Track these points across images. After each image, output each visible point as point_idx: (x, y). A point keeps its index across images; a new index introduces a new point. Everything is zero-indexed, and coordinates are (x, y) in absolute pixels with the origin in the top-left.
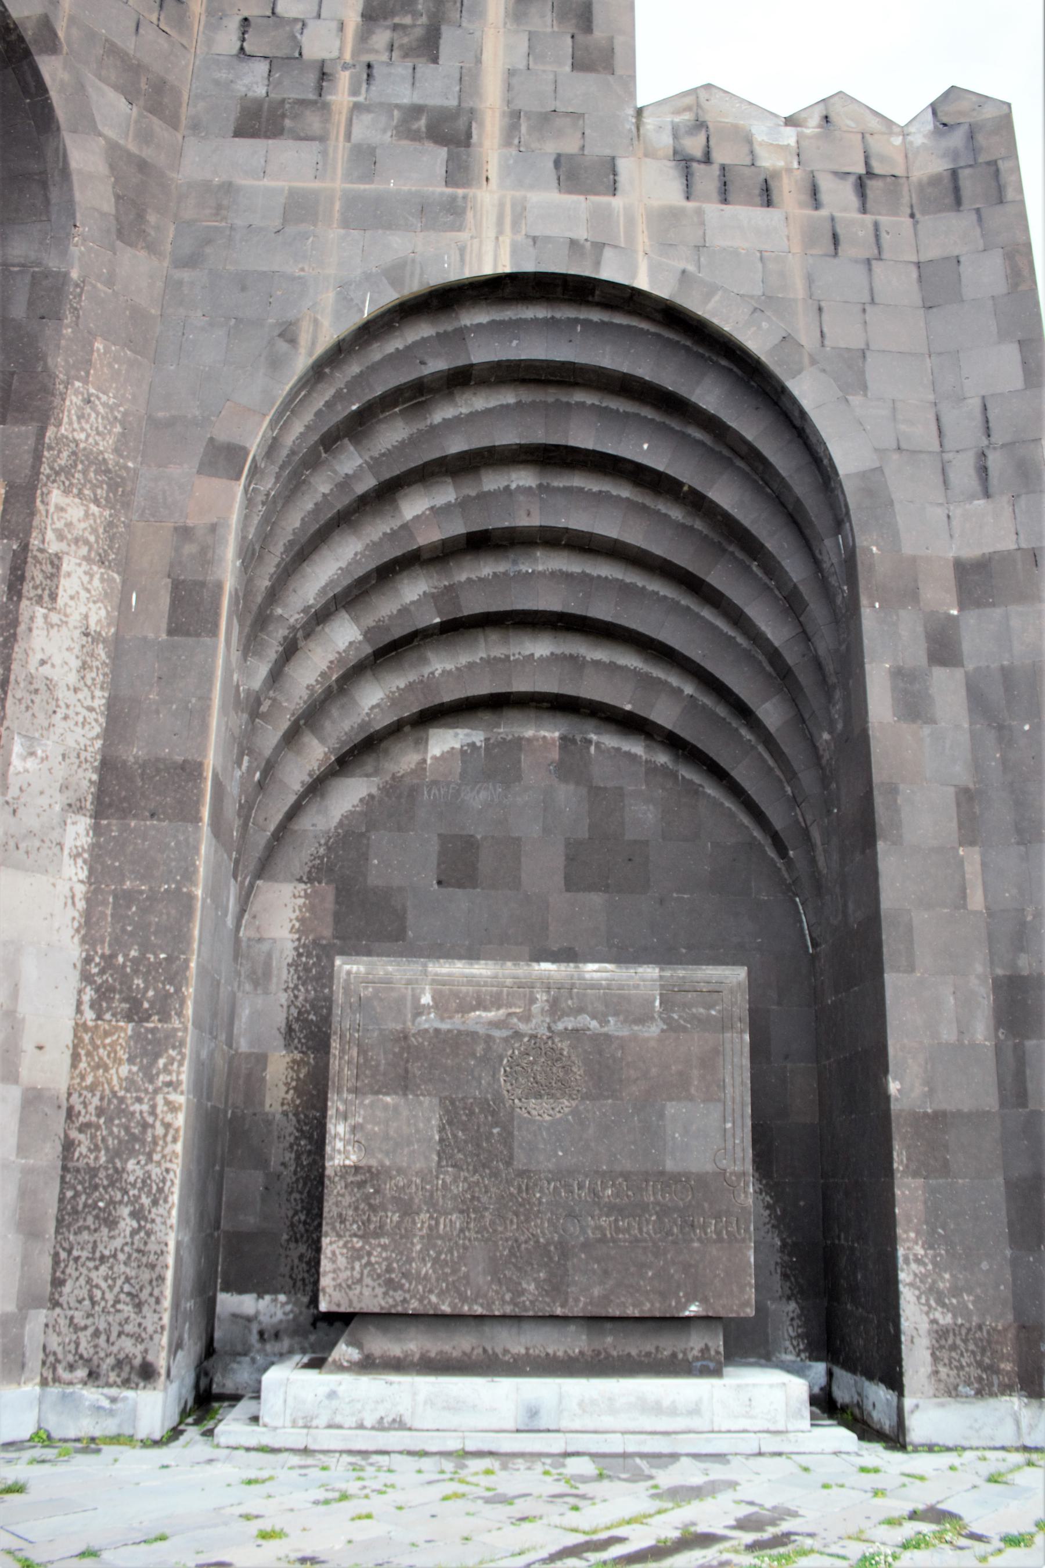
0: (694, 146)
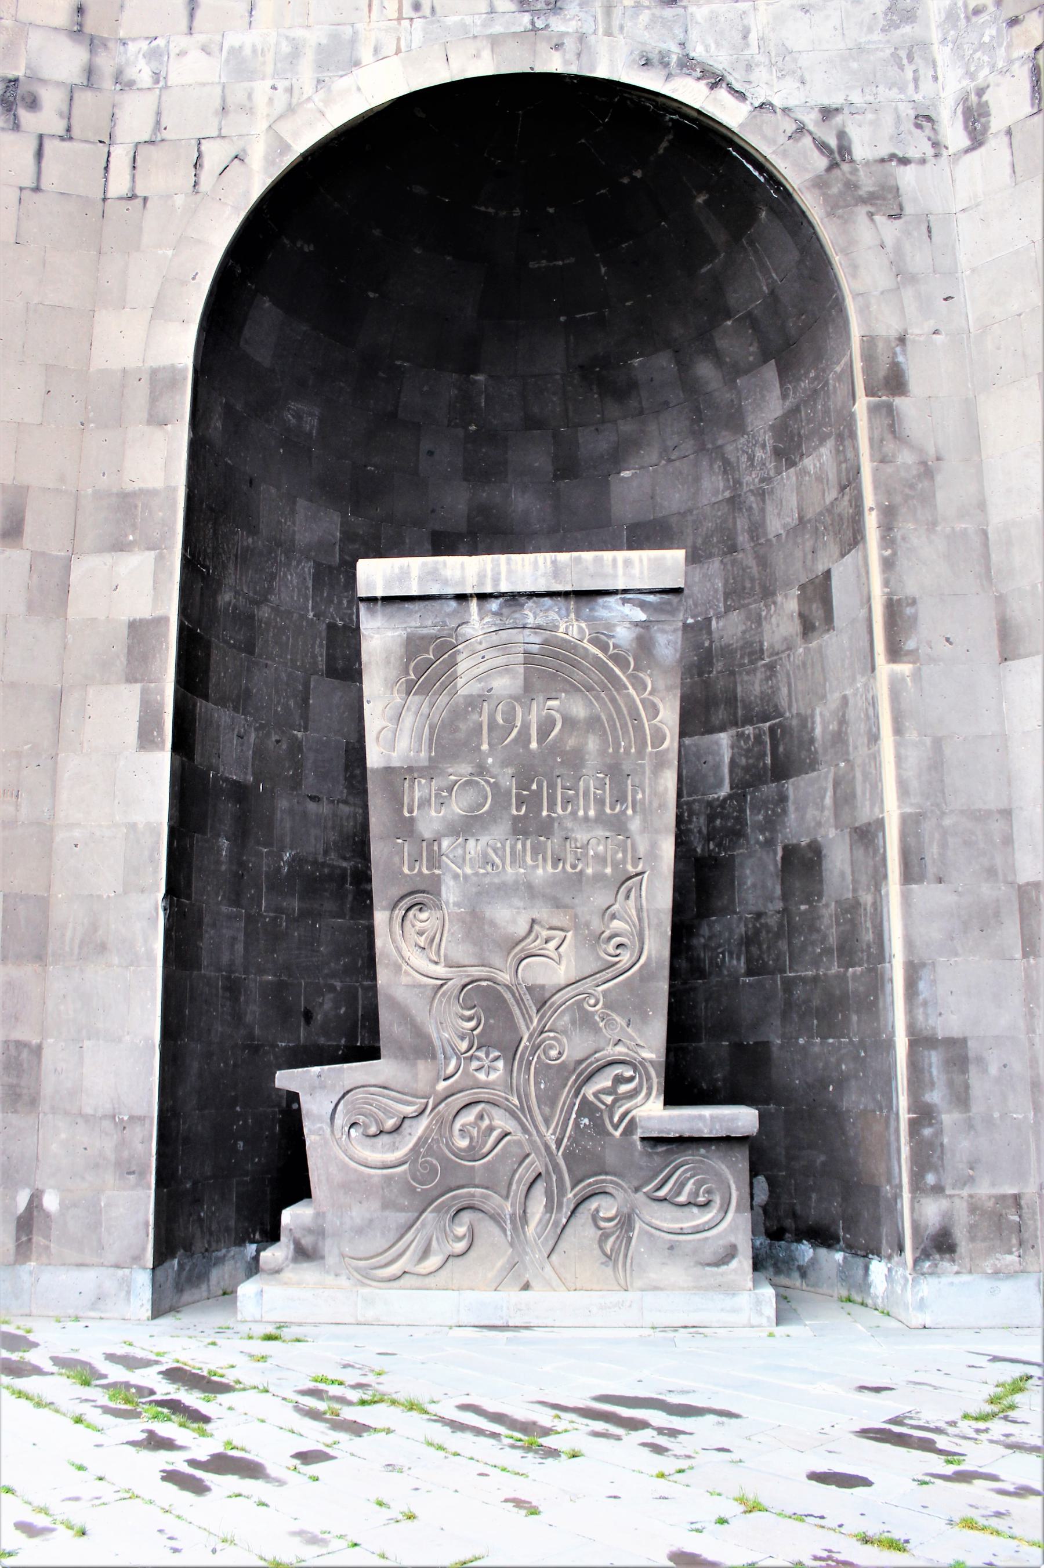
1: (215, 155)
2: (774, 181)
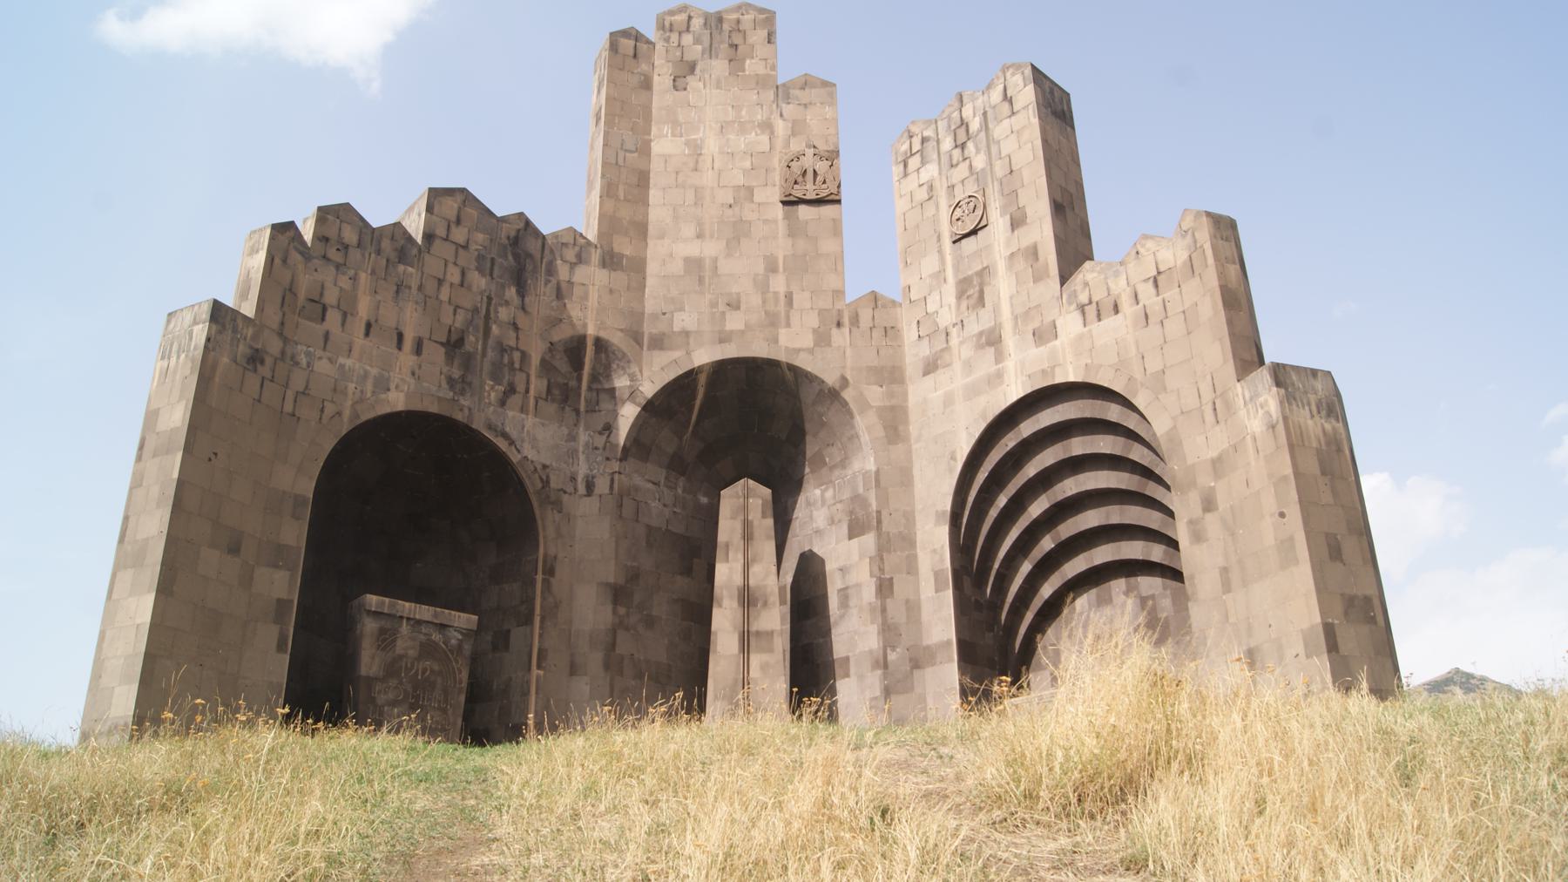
0: (1083, 298)
1: (330, 409)
2: (521, 483)
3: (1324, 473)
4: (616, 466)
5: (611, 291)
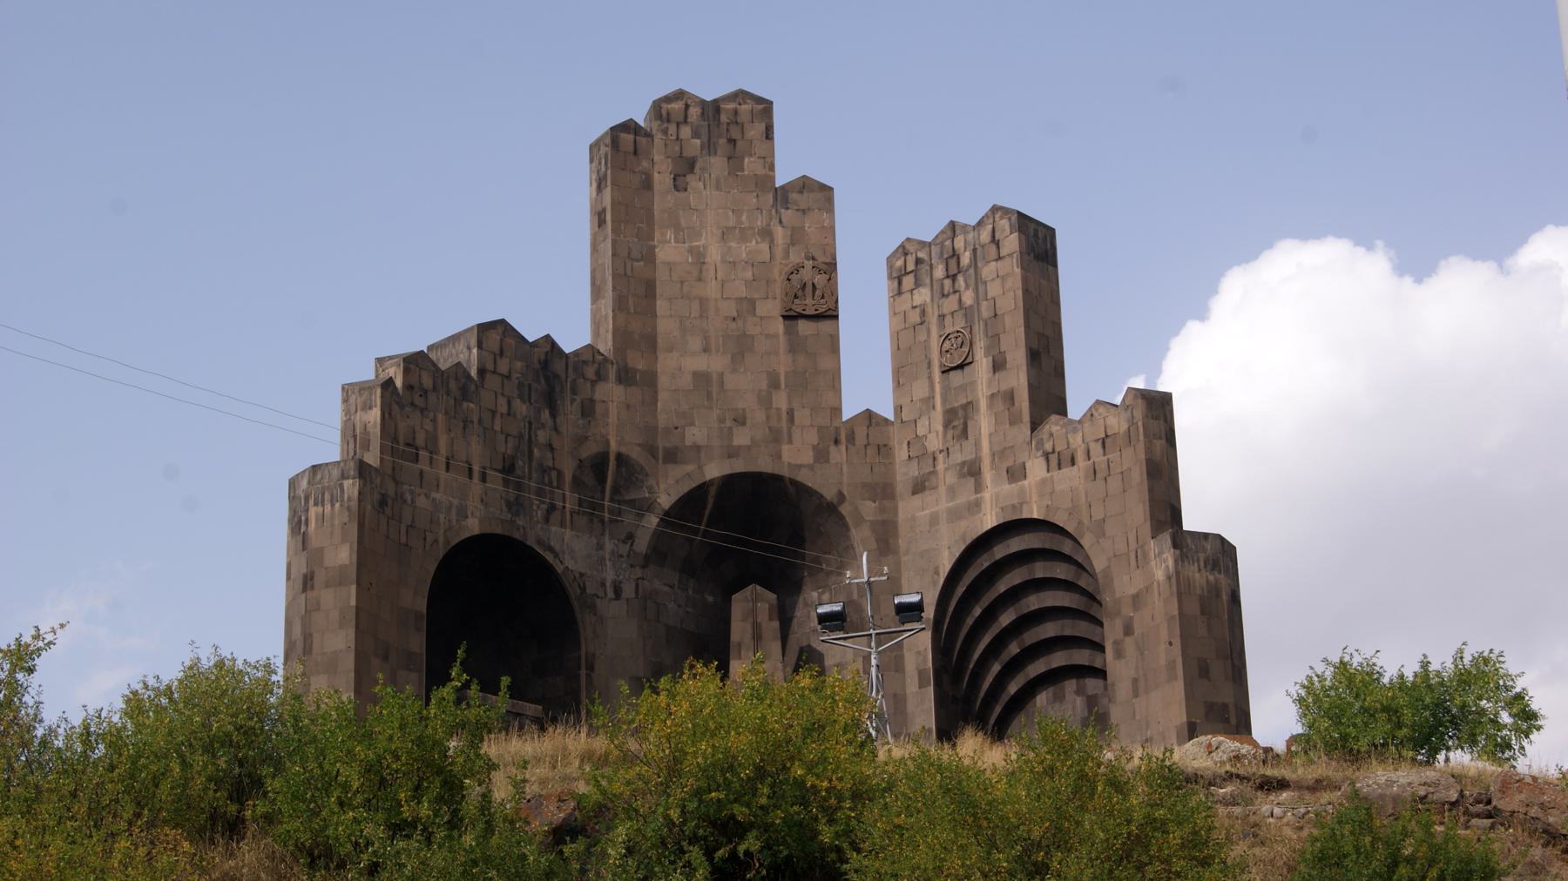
0: (1048, 447)
1: (430, 538)
3: (1203, 613)
4: (638, 572)
5: (628, 407)
